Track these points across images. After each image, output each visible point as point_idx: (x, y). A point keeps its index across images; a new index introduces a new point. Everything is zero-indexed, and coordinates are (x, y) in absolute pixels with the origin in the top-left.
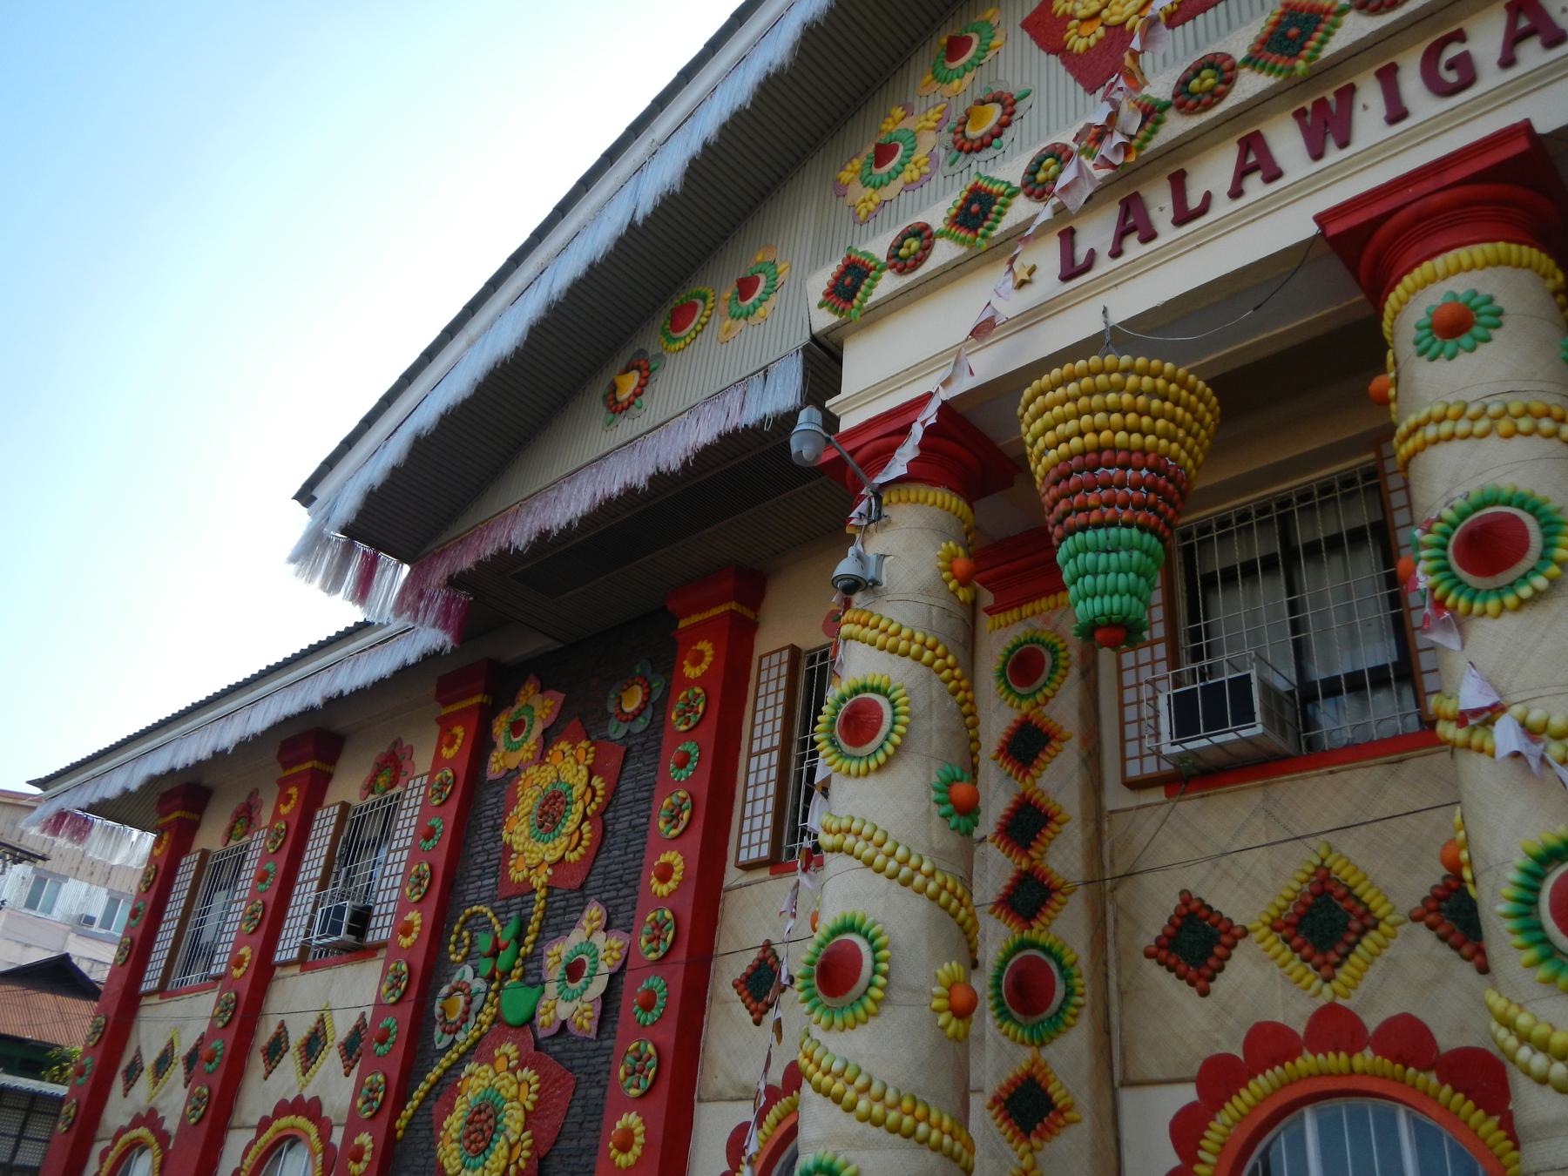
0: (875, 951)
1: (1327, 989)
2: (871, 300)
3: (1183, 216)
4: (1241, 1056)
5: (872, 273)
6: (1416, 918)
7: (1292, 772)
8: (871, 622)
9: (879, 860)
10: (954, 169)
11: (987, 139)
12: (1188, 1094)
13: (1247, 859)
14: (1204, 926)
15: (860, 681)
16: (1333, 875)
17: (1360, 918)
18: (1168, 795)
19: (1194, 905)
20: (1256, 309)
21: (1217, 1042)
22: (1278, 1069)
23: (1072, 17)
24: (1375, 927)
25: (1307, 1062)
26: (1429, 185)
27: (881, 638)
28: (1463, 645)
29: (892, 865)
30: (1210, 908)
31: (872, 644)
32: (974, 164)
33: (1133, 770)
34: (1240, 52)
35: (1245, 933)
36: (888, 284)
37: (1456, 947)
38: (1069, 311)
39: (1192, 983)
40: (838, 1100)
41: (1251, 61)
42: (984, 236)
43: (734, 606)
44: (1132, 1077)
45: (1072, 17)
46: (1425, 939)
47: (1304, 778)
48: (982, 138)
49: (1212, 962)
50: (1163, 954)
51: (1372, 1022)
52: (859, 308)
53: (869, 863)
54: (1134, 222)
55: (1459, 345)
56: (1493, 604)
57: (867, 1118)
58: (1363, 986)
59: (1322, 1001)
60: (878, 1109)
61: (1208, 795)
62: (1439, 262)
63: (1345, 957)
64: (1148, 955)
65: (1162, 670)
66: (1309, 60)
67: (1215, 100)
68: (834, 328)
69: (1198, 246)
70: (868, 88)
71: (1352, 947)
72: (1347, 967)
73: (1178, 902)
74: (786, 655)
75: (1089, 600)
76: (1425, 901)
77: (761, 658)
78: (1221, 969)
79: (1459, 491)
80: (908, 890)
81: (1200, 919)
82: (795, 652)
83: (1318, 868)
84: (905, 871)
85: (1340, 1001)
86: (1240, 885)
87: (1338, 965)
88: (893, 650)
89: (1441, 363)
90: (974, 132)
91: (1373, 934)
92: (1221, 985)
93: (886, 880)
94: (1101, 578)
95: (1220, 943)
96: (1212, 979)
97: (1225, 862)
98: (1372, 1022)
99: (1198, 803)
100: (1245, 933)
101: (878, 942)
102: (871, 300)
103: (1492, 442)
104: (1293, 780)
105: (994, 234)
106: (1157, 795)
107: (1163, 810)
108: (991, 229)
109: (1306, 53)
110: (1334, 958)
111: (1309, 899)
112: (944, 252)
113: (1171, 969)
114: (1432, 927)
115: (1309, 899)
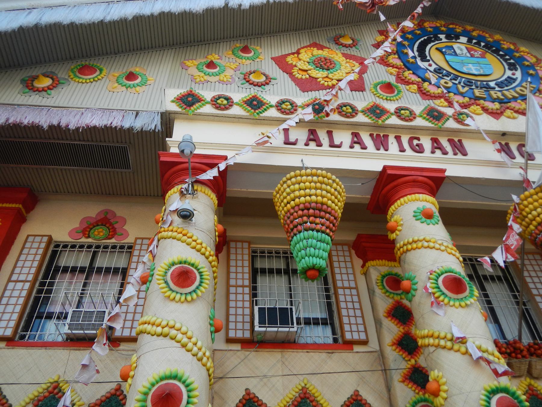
0: (189, 391)
2: (199, 111)
3: (332, 145)
5: (203, 102)
7: (293, 349)
8: (188, 235)
9: (190, 345)
10: (243, 86)
11: (260, 84)
13: (274, 380)
14: (255, 405)
15: (184, 259)
16: (308, 391)
18: (242, 348)
19: (252, 396)
20: (362, 184)
23: (295, 66)
26: (419, 173)
28: (445, 313)
29: (195, 349)
30: (258, 398)
31: (188, 244)
32: (252, 89)
33: (232, 334)
34: (360, 109)
36: (208, 109)
38: (279, 154)
41: (364, 112)
42: (258, 114)
43: (21, 206)
45: (295, 66)
47: (297, 352)
48: (258, 83)
52: (193, 111)
53: (184, 346)
54: (313, 137)
55: (426, 221)
56: (457, 304)
61: (259, 351)
62: (421, 196)
65: (247, 297)
66: (383, 122)
67: (351, 116)
68: (176, 113)
69: (338, 156)
70: (201, 41)
73: (244, 393)
74: (45, 239)
75: (311, 257)
77: (28, 236)
80: (199, 363)
81: (254, 402)
82: (50, 238)
83: (303, 388)
84: (200, 354)
86: (270, 390)
88: (198, 251)
90: (252, 78)
93: (192, 356)
94: (317, 250)
97: (265, 380)
99: (254, 353)
101: (191, 387)
102: (199, 111)
103: (445, 253)
104: (293, 352)
105: (261, 115)
106: (238, 347)
107: (239, 353)
108: (261, 113)
109: (382, 119)
111: (299, 400)
112: (235, 110)
115: (299, 400)
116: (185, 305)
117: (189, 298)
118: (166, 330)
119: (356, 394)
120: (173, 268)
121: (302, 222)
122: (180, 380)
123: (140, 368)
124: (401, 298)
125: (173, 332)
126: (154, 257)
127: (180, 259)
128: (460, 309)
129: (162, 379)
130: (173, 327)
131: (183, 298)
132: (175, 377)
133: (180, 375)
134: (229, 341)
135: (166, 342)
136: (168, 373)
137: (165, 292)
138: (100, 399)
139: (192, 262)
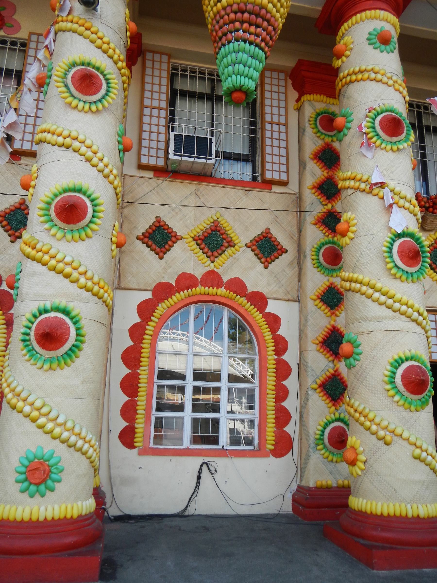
1: (212, 264)
4: (174, 285)
6: (247, 246)
7: (209, 183)
8: (92, 29)
9: (95, 160)
12: (148, 295)
13: (186, 210)
14: (165, 232)
15: (87, 60)
16: (219, 225)
17: (228, 242)
18: (155, 176)
19: (162, 223)
21: (163, 277)
22: (190, 290)
24: (234, 246)
25: (200, 289)
27: (99, 42)
28: (373, 157)
29: (101, 165)
31: (93, 42)
33: (144, 160)
35: (182, 238)
37: (259, 259)
39: (157, 253)
40: (67, 276)
44: (122, 285)
46: (249, 253)
47: (213, 186)
49: (167, 247)
50: (146, 240)
51: (225, 279)
53: (89, 160)
55: (380, 47)
56: (389, 147)
57: (84, 287)
58: (224, 266)
59: (208, 269)
60: (90, 284)
61: (172, 181)
63: (220, 255)
64: (138, 238)
65: (163, 122)
71: (224, 251)
72: (220, 258)
73: (155, 220)
75: (239, 76)
76: (251, 241)
78: (169, 250)
79: (381, 102)
80: (106, 180)
81: (164, 229)
83: (215, 221)
84: (107, 171)
85: (215, 270)
86: (181, 220)
87: (216, 257)
88: (105, 52)
89: (377, 51)
91: (232, 248)
92: (168, 256)
93: (97, 172)
94: (247, 68)
95: (171, 240)
96: (165, 253)
97: (177, 209)
98: (225, 279)
99: (167, 183)
100: (182, 238)
101: (96, 202)
103: (392, 89)
104: (209, 185)
106: (150, 174)
110: (216, 254)
111: (210, 231)
113: (148, 246)
114: (253, 250)
115: (210, 231)
116: (89, 116)
117: (94, 108)
118: (68, 141)
119: (268, 231)
120: (74, 70)
121: (233, 30)
122: (84, 194)
123: (41, 178)
124: (332, 141)
125: (76, 144)
126: (51, 54)
127: (82, 59)
128: (391, 153)
129: (65, 191)
130: (76, 139)
131: (87, 107)
132: (80, 191)
133: (84, 189)
134: (141, 167)
135: (69, 153)
136: (71, 186)
137: (65, 98)
138: (5, 211)
139: (97, 65)
